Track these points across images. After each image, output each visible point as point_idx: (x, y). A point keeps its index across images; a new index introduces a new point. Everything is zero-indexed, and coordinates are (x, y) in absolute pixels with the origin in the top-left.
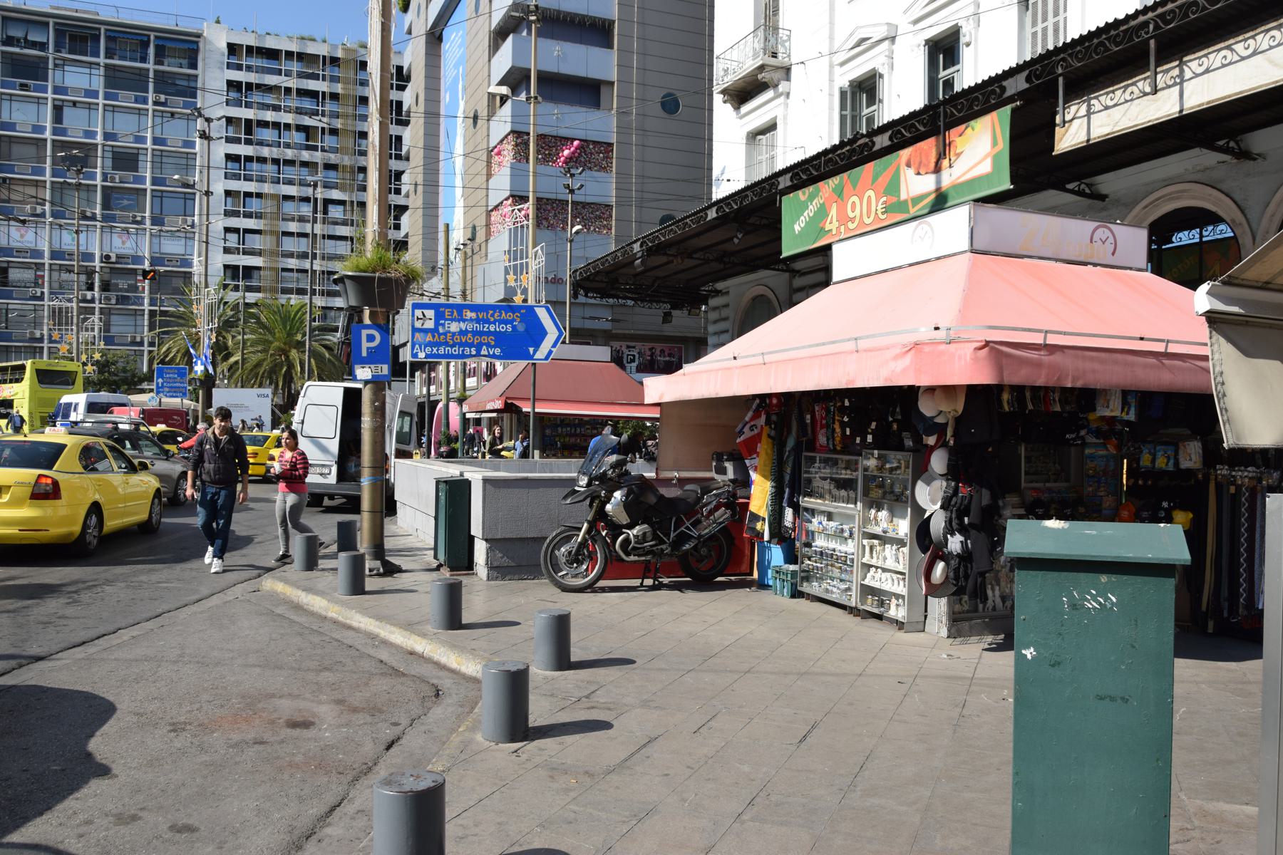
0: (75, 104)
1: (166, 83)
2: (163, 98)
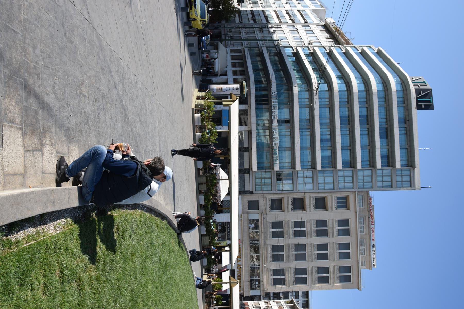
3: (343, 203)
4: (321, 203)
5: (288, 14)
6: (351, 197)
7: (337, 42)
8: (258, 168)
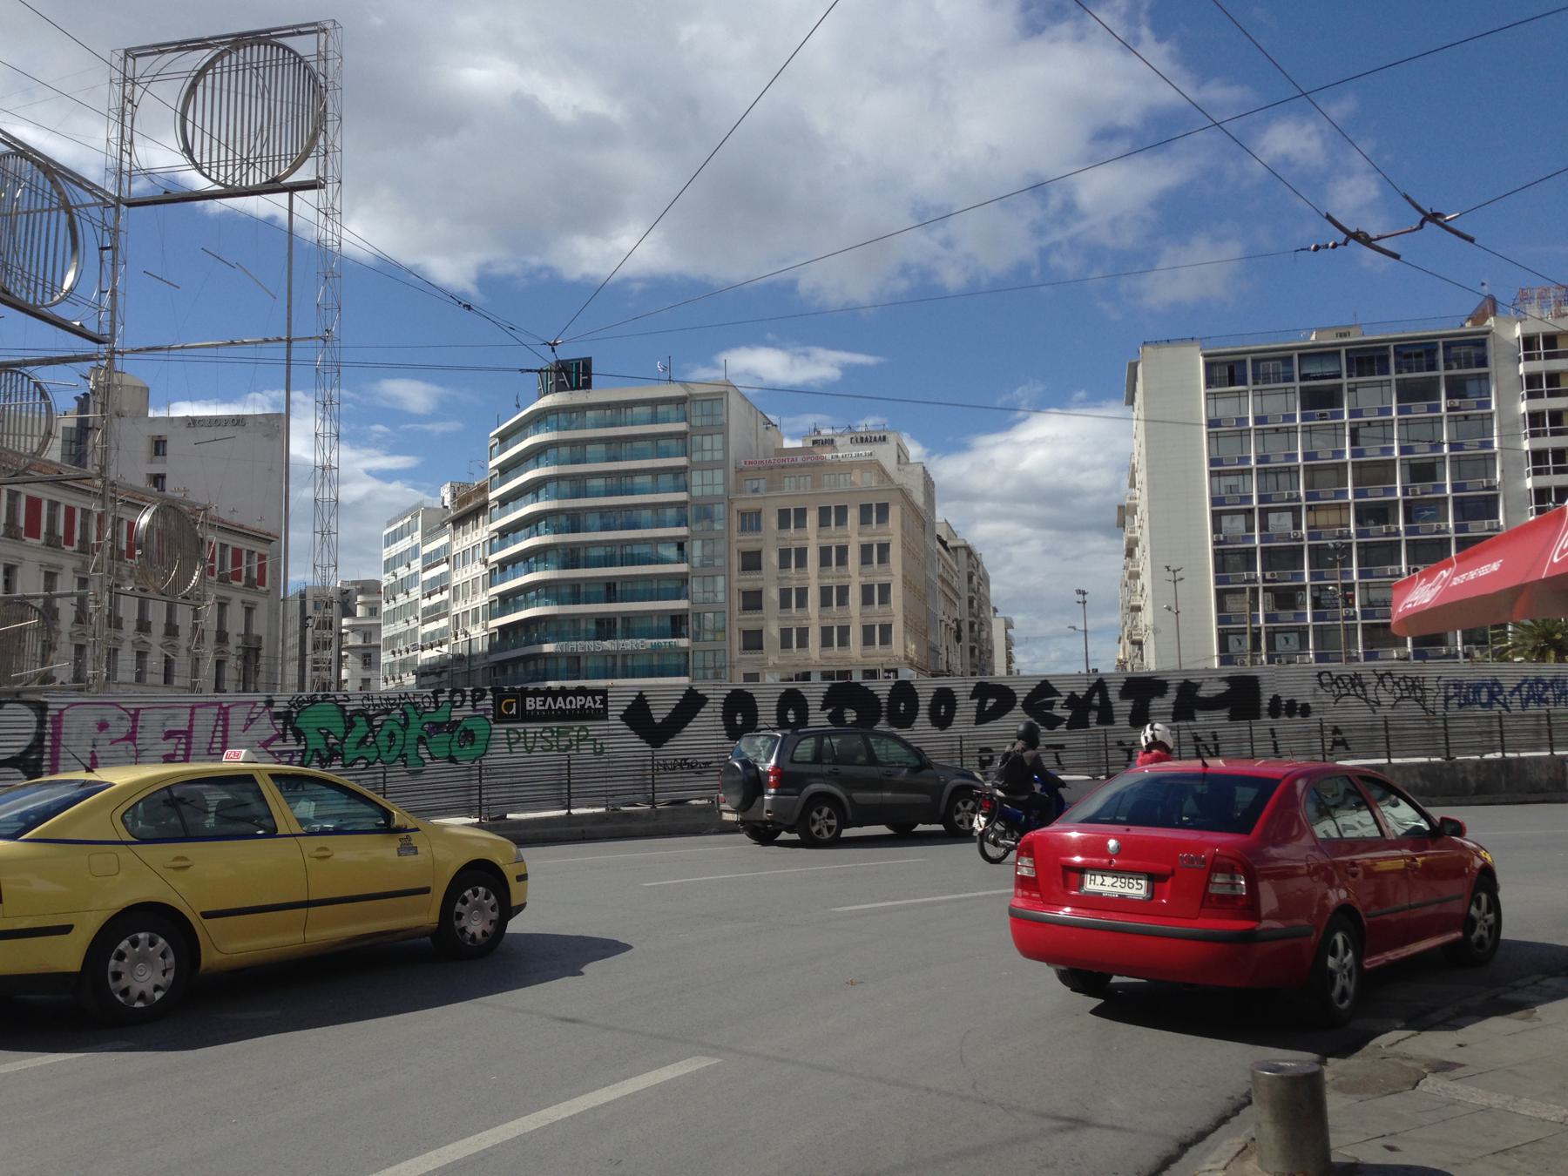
0: (1369, 423)
1: (1457, 389)
2: (1457, 402)
3: (751, 521)
4: (752, 561)
5: (429, 596)
6: (739, 505)
7: (481, 509)
8: (686, 674)
